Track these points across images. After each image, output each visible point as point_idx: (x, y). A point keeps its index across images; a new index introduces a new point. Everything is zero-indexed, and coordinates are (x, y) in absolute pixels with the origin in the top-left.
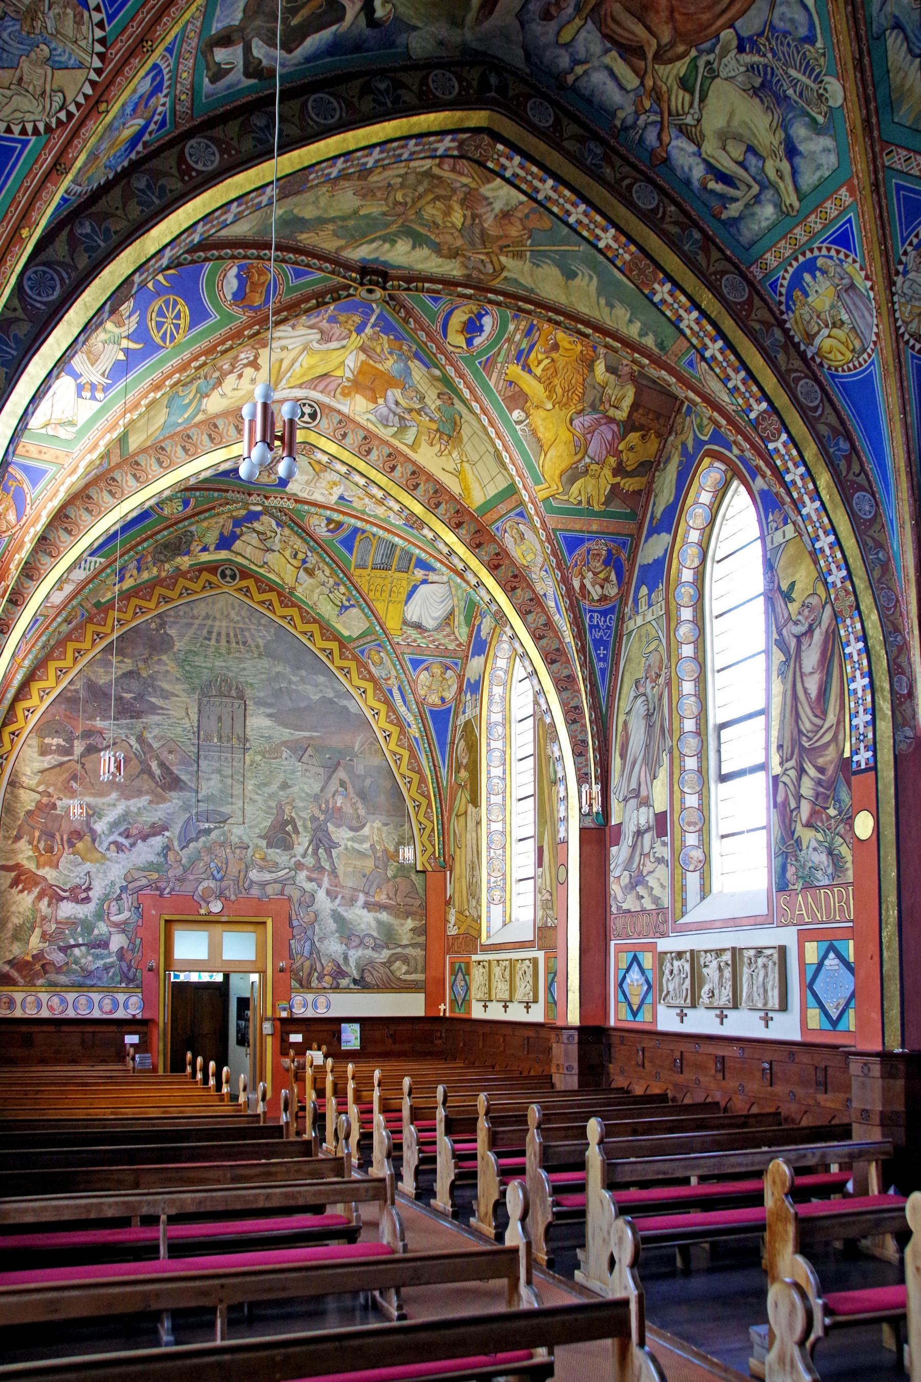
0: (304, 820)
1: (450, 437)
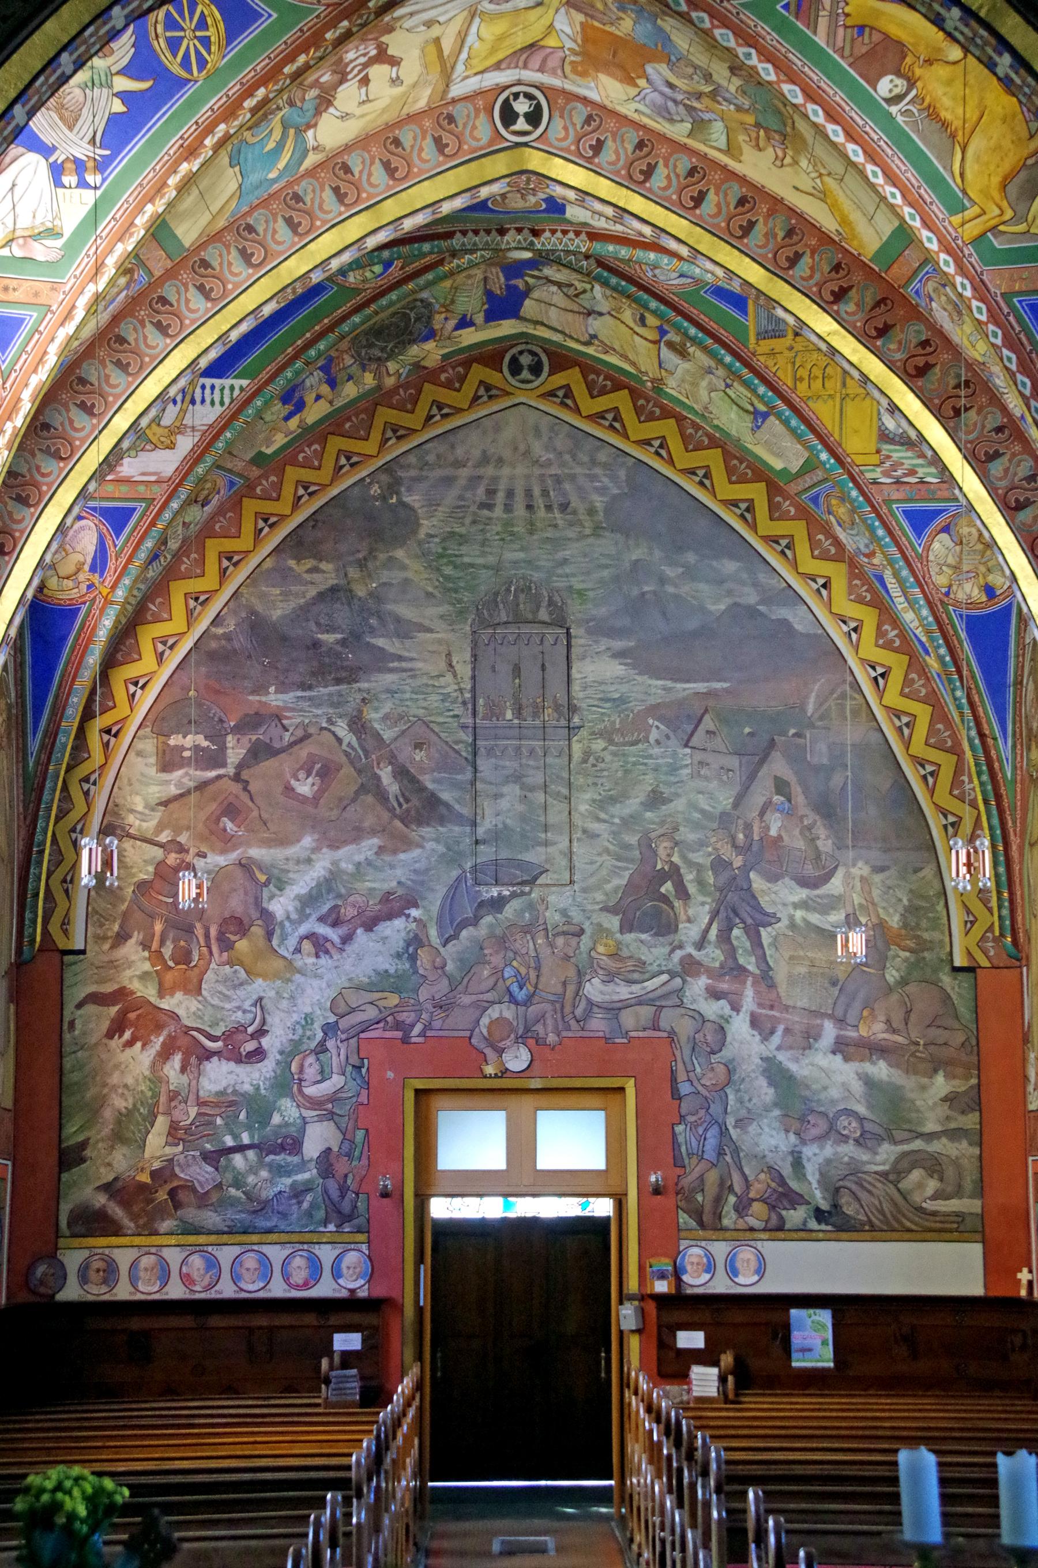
0: (699, 868)
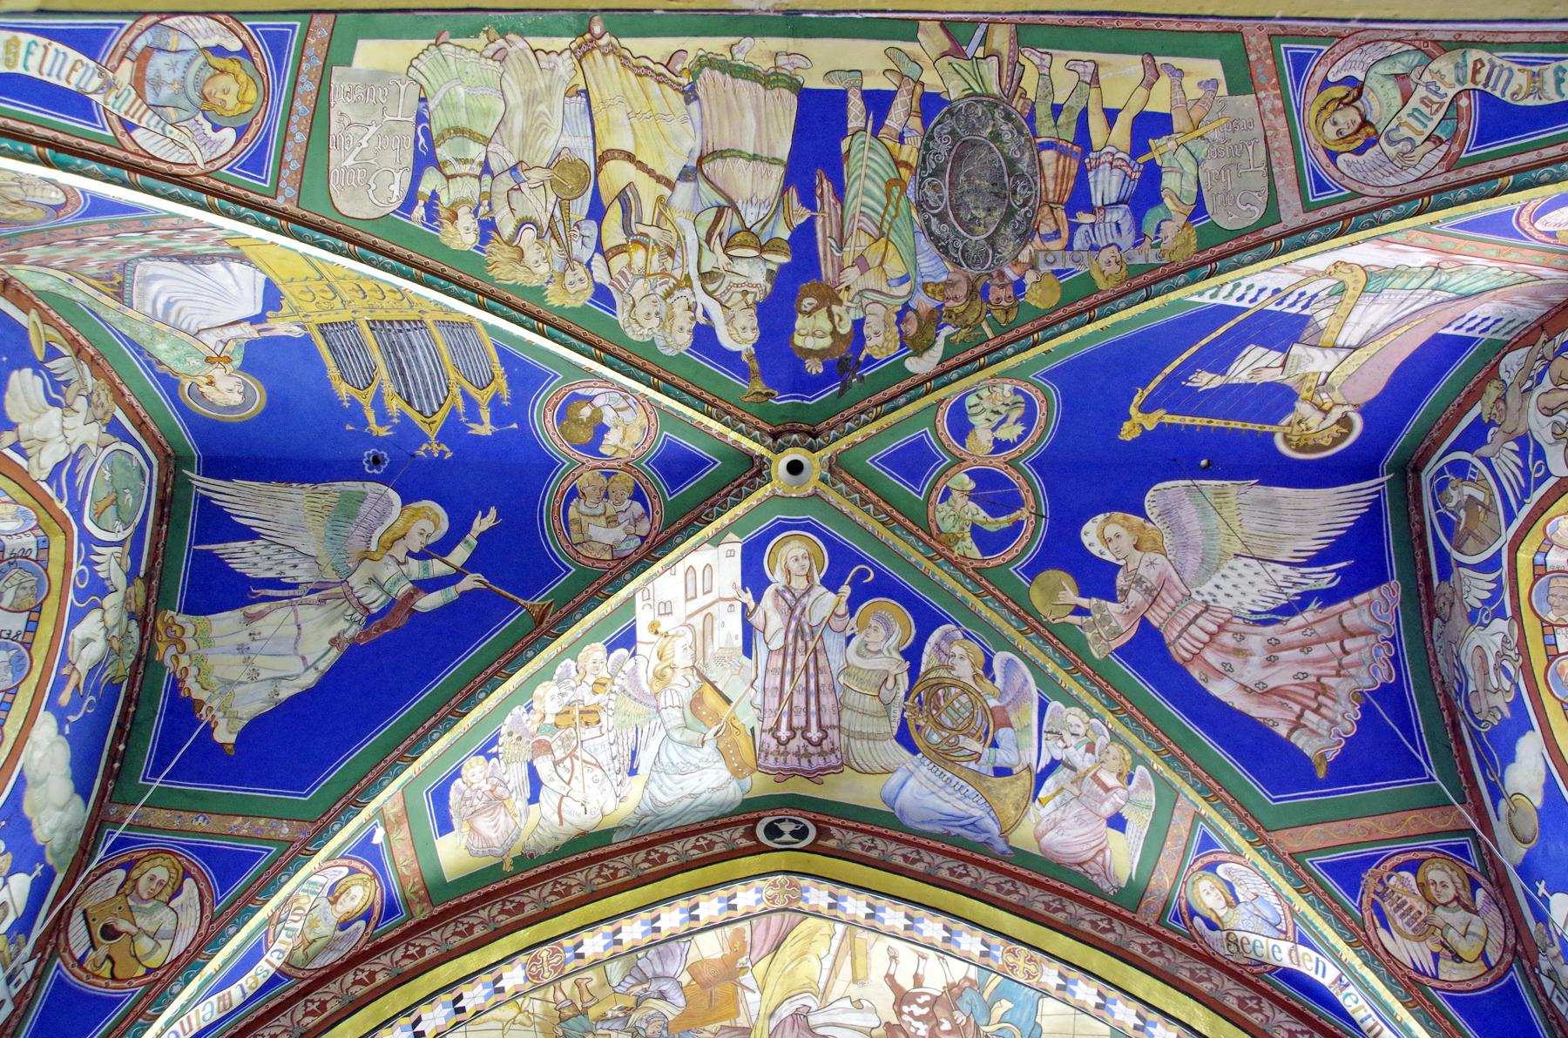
1: (562, 1020)
